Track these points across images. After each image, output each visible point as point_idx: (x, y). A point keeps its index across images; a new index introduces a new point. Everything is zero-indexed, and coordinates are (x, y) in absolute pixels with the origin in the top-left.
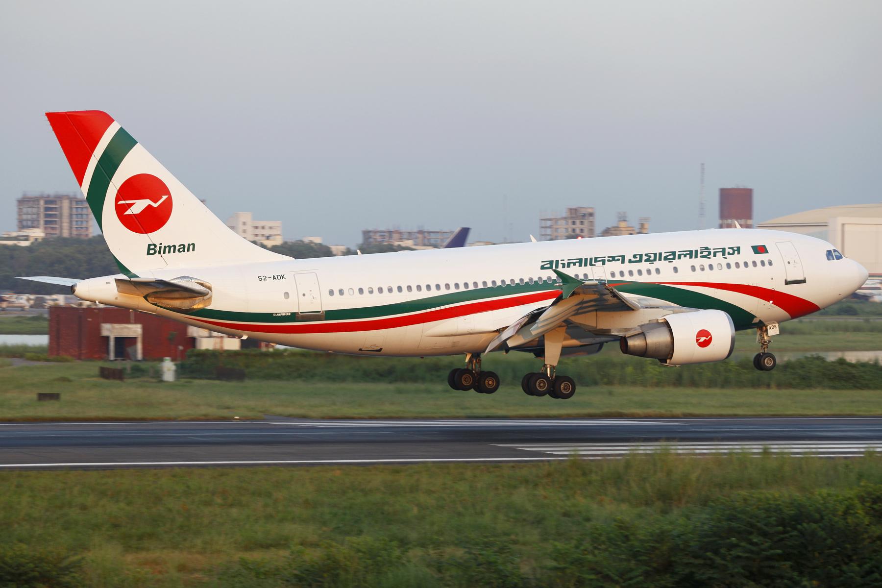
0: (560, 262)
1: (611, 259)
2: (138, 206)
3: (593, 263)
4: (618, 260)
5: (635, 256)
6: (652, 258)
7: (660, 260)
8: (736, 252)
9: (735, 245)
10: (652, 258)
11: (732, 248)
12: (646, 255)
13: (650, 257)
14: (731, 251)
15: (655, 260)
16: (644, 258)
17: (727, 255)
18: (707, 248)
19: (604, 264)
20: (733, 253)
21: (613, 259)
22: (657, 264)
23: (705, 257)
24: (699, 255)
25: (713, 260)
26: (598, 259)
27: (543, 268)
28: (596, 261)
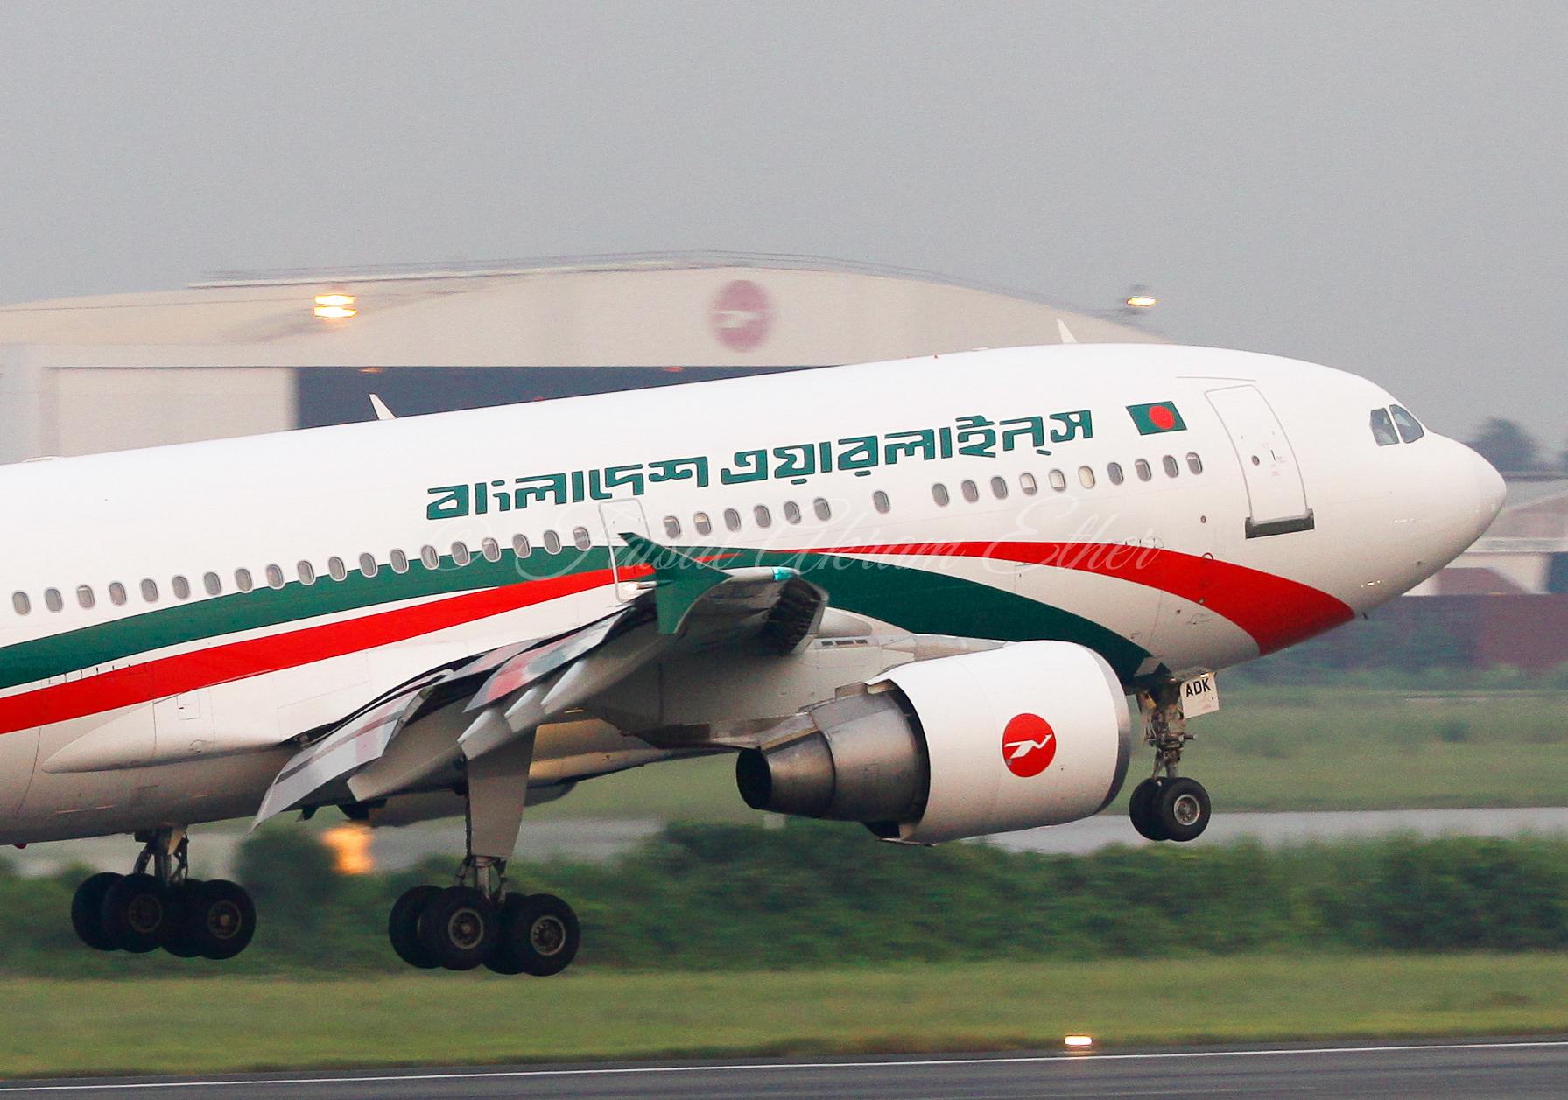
0: (491, 490)
1: (660, 471)
3: (604, 489)
4: (687, 474)
5: (740, 459)
6: (799, 464)
7: (826, 468)
8: (1079, 430)
9: (1072, 404)
10: (799, 464)
12: (779, 452)
13: (793, 458)
14: (1062, 428)
15: (809, 469)
16: (774, 463)
17: (1049, 444)
18: (979, 421)
19: (639, 490)
20: (1070, 436)
21: (669, 470)
22: (818, 483)
23: (977, 451)
24: (956, 445)
25: (1003, 463)
26: (619, 475)
27: (434, 512)
28: (612, 481)
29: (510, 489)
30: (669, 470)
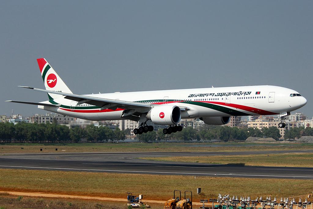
0: (195, 95)
2: (51, 81)
5: (218, 94)
11: (248, 92)
14: (247, 93)
21: (211, 94)
22: (223, 97)
23: (239, 95)
24: (237, 94)
25: (241, 96)
27: (189, 97)
29: (196, 95)
30: (211, 94)
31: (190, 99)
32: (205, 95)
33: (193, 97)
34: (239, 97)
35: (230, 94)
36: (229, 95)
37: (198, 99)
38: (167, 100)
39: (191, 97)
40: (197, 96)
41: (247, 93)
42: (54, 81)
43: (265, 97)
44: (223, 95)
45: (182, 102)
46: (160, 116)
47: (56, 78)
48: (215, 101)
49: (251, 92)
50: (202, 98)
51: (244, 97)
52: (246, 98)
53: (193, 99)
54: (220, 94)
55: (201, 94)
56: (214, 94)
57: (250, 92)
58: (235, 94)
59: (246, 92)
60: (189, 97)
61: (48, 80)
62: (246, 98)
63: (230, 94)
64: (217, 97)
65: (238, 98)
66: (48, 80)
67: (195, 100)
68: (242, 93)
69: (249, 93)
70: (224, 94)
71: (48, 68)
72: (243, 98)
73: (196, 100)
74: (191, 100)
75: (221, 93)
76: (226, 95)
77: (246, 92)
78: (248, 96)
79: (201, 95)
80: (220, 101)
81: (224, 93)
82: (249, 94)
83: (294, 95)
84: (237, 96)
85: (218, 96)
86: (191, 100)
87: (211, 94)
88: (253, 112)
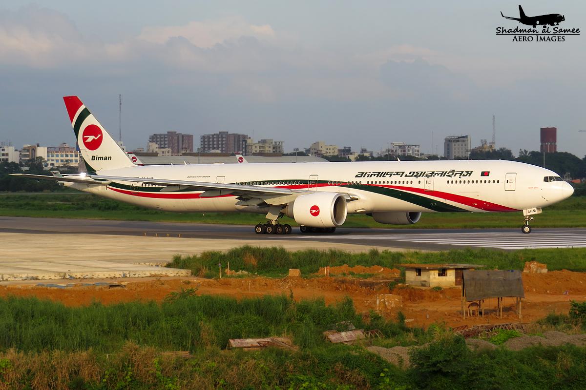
2: (91, 138)
5: (410, 173)
9: (469, 170)
11: (467, 172)
14: (466, 174)
22: (420, 178)
23: (449, 176)
24: (447, 174)
25: (454, 178)
27: (357, 176)
30: (397, 174)
31: (358, 180)
32: (387, 174)
33: (364, 176)
34: (450, 179)
35: (433, 174)
36: (431, 176)
37: (375, 180)
38: (316, 181)
39: (361, 176)
40: (372, 175)
41: (466, 174)
42: (96, 139)
43: (498, 182)
44: (420, 176)
45: (344, 184)
46: (311, 212)
47: (101, 133)
48: (405, 185)
49: (472, 172)
50: (381, 179)
51: (460, 179)
52: (462, 182)
53: (364, 181)
54: (414, 173)
55: (379, 173)
56: (403, 173)
57: (469, 172)
58: (443, 174)
59: (463, 172)
60: (357, 176)
61: (85, 137)
62: (462, 182)
63: (433, 174)
64: (409, 179)
65: (448, 182)
66: (85, 137)
67: (368, 182)
68: (455, 173)
69: (469, 173)
70: (422, 174)
71: (85, 113)
72: (458, 182)
73: (370, 183)
74: (360, 182)
75: (417, 173)
76: (427, 176)
77: (463, 172)
78: (467, 178)
79: (379, 174)
80: (415, 185)
81: (422, 172)
82: (469, 176)
83: (551, 178)
84: (446, 178)
85: (412, 176)
86: (360, 182)
87: (397, 173)
88: (474, 206)
